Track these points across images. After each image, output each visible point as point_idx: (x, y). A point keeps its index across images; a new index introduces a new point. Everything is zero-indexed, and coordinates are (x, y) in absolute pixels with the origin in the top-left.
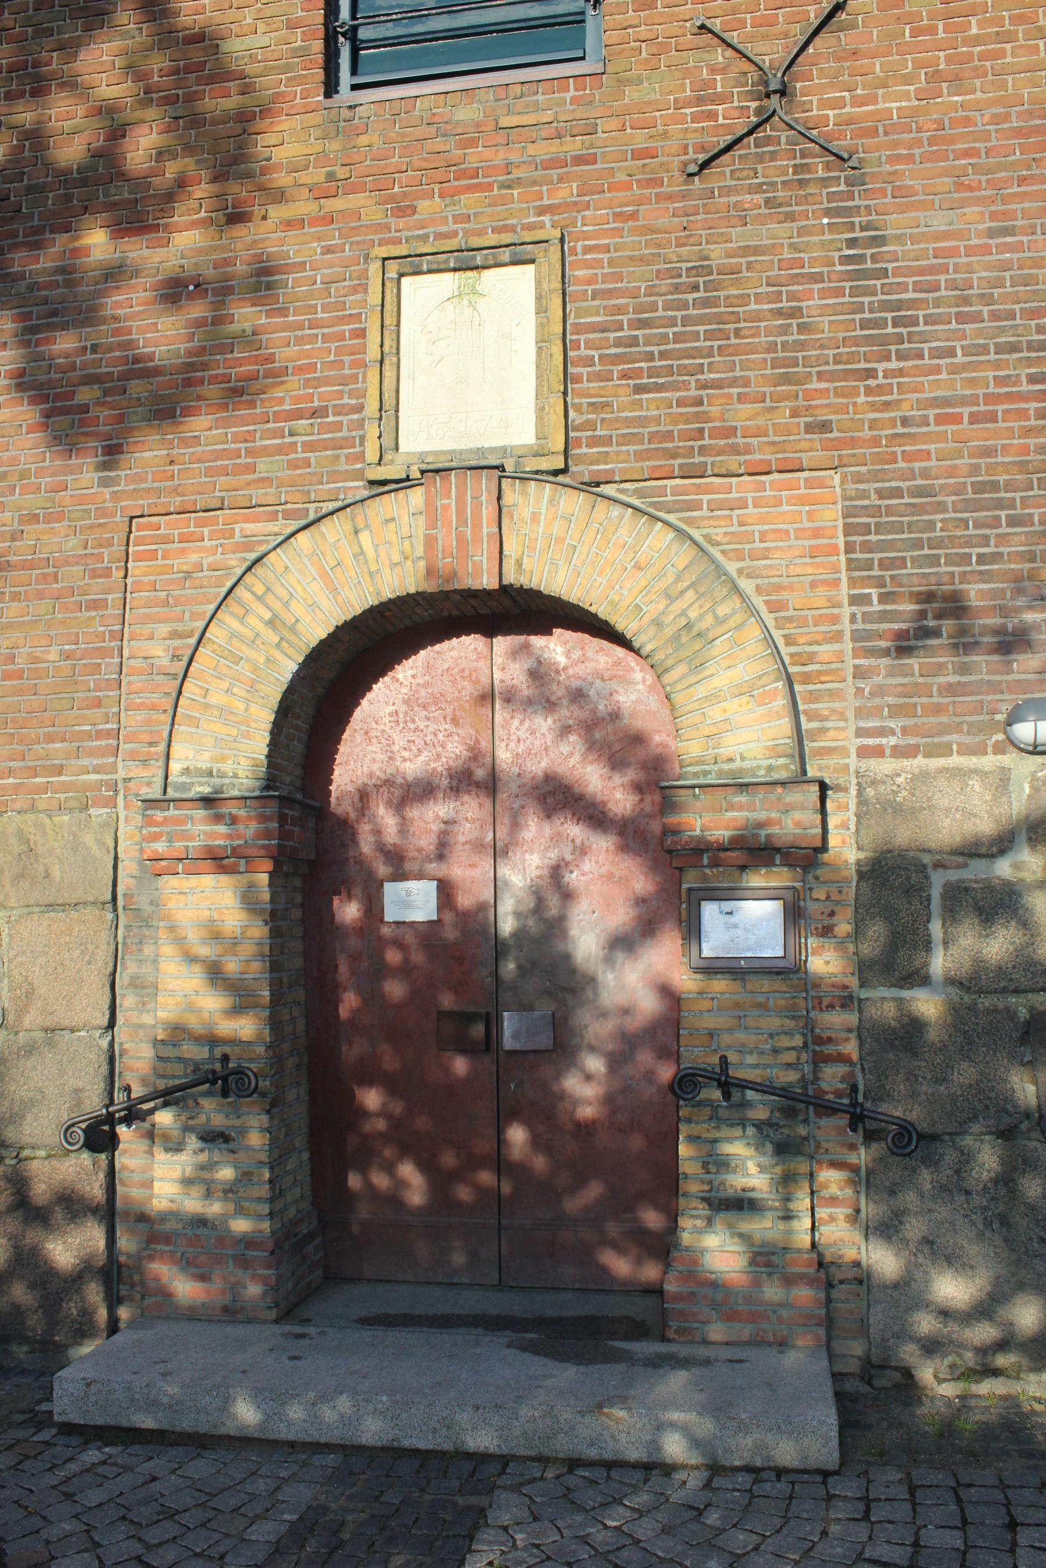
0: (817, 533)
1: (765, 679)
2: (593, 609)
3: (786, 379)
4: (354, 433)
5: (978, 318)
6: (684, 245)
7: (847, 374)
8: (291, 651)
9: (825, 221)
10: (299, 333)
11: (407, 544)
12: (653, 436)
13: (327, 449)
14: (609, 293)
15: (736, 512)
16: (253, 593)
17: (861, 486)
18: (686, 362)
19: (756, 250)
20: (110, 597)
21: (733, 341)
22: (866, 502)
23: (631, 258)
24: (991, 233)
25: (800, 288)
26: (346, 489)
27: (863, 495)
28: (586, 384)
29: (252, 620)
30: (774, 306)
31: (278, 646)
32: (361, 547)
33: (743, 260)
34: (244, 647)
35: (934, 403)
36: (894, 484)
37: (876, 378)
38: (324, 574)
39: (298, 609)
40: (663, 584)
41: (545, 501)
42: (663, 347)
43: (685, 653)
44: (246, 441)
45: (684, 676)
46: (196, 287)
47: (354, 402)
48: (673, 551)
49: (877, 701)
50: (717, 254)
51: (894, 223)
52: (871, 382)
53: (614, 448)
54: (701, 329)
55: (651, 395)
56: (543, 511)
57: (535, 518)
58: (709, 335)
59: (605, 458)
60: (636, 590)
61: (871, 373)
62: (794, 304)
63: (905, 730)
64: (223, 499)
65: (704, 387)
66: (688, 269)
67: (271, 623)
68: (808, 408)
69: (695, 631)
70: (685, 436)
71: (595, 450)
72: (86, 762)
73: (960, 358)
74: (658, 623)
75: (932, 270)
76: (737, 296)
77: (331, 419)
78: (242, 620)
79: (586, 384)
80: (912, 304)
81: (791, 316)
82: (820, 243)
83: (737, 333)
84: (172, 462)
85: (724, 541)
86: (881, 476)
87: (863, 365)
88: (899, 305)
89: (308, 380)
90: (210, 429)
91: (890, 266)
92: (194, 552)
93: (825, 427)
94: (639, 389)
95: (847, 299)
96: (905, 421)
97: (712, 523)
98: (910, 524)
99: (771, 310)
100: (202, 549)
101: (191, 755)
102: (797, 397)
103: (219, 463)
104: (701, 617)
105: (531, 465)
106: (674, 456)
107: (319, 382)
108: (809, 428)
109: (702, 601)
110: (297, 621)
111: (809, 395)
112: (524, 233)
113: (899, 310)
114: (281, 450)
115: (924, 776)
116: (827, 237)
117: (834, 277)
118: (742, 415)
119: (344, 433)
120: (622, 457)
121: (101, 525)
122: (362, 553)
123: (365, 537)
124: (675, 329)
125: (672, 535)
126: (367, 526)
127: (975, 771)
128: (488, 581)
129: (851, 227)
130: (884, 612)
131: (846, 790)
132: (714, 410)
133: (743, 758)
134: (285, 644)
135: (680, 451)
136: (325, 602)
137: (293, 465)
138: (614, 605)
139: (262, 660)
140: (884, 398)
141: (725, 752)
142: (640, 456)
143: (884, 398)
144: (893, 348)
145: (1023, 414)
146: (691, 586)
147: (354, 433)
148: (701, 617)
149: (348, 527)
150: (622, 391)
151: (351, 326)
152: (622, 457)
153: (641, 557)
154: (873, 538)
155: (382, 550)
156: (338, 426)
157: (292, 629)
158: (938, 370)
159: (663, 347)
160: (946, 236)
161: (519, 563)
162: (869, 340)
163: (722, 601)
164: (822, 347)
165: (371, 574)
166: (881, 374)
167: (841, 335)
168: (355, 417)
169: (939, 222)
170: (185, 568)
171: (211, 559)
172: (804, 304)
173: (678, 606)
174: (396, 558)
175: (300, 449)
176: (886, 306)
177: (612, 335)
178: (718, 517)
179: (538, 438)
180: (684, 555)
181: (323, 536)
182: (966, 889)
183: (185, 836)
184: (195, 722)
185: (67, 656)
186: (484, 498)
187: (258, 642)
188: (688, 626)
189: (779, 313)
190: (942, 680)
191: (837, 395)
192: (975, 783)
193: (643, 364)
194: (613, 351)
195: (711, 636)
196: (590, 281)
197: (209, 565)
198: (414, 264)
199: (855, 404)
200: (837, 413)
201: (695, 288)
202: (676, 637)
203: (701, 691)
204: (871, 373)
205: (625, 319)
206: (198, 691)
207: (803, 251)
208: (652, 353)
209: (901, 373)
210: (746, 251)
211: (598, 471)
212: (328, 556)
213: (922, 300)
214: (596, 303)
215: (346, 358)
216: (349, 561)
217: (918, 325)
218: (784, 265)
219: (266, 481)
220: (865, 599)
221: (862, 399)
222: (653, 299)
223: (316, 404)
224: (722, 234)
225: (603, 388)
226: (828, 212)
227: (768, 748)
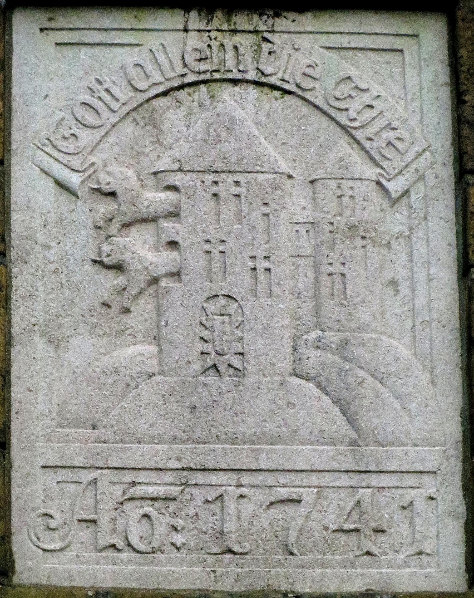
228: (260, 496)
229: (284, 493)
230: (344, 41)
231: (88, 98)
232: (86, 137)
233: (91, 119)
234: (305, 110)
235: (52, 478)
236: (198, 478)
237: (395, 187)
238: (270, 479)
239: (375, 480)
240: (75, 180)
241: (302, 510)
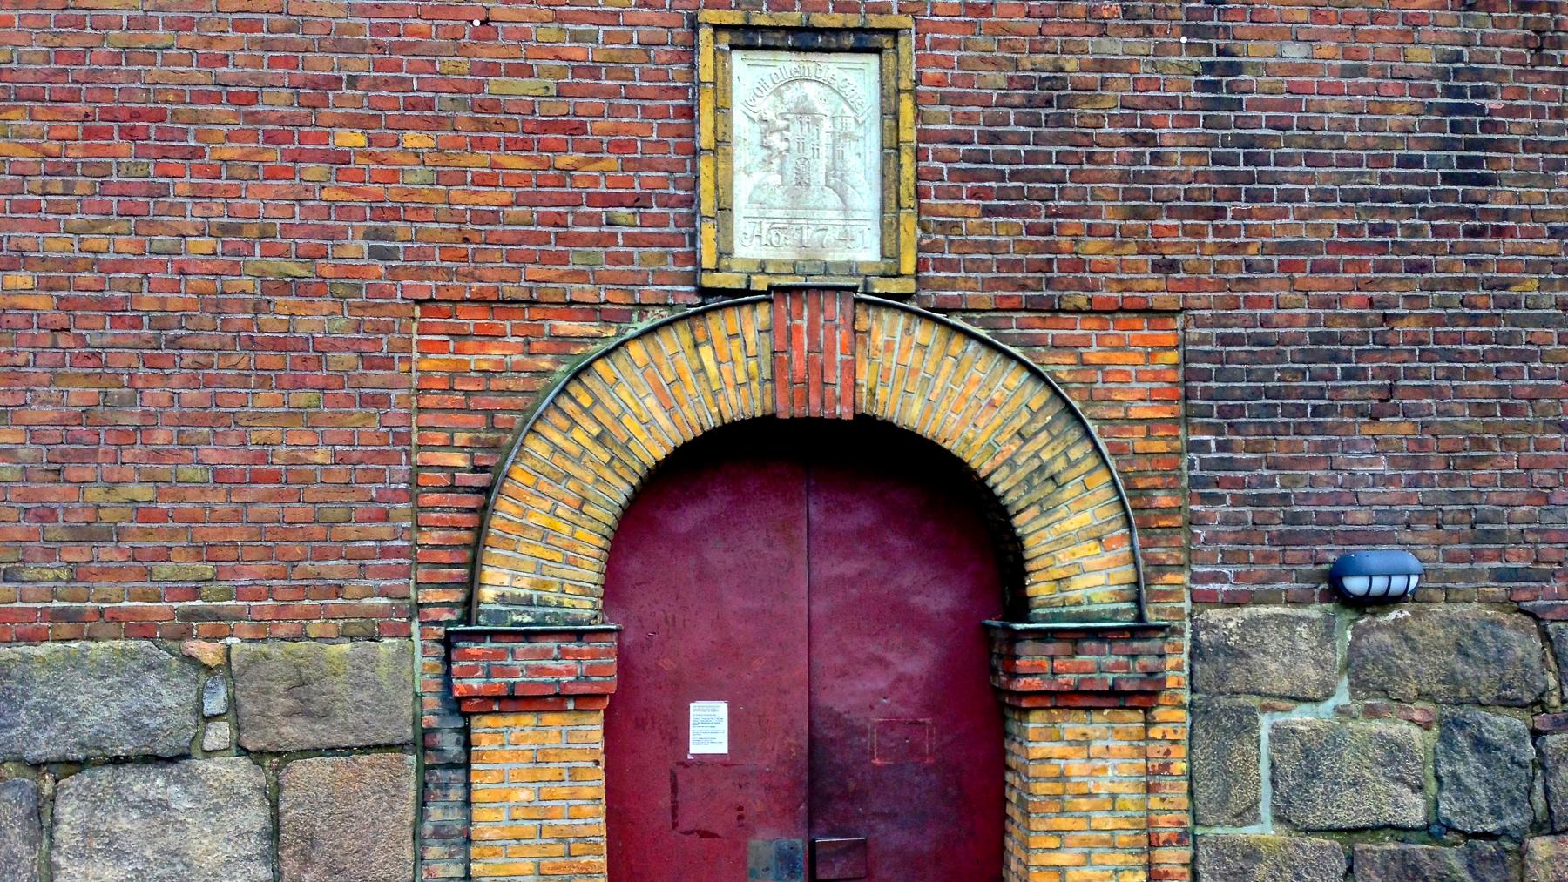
0: (1157, 376)
1: (1113, 525)
2: (946, 446)
3: (1137, 213)
4: (683, 230)
5: (1324, 161)
6: (1039, 52)
7: (1196, 213)
8: (624, 473)
9: (1184, 40)
10: (615, 102)
11: (752, 363)
12: (1001, 265)
13: (651, 245)
14: (960, 100)
17: (1204, 331)
18: (1038, 185)
19: (1113, 66)
20: (393, 393)
21: (1086, 167)
22: (1207, 348)
23: (983, 59)
24: (1345, 72)
25: (1155, 113)
26: (674, 293)
27: (1204, 340)
28: (934, 201)
29: (578, 434)
30: (1128, 131)
31: (608, 465)
32: (701, 362)
33: (1098, 76)
34: (568, 464)
35: (1281, 248)
36: (1236, 330)
37: (1225, 218)
38: (658, 391)
40: (1017, 424)
41: (900, 329)
42: (1015, 167)
43: (1036, 495)
44: (556, 225)
45: (1035, 518)
46: (482, 23)
47: (682, 193)
49: (1211, 548)
50: (1071, 64)
51: (1253, 51)
52: (1219, 222)
53: (963, 274)
54: (1053, 149)
55: (1001, 219)
56: (898, 339)
57: (889, 346)
59: (951, 284)
60: (990, 428)
62: (1149, 130)
63: (1237, 575)
64: (531, 291)
65: (1055, 215)
66: (1043, 80)
67: (598, 439)
68: (1157, 245)
69: (1047, 474)
70: (1034, 267)
71: (942, 274)
72: (371, 583)
73: (1307, 205)
74: (1011, 463)
75: (1283, 106)
76: (1090, 116)
77: (655, 210)
78: (564, 432)
79: (934, 201)
80: (1264, 141)
81: (1144, 144)
82: (1179, 67)
83: (1090, 157)
84: (466, 240)
86: (1223, 321)
87: (1211, 204)
88: (1251, 142)
89: (628, 160)
90: (512, 205)
91: (1245, 97)
93: (1172, 266)
94: (988, 211)
95: (1200, 130)
96: (1249, 267)
98: (1249, 372)
99: (1125, 135)
100: (506, 346)
101: (507, 581)
102: (1146, 234)
103: (524, 247)
104: (1054, 459)
105: (881, 286)
106: (1024, 287)
107: (640, 165)
108: (1156, 267)
111: (1157, 231)
112: (871, 16)
113: (1252, 146)
114: (598, 240)
115: (1253, 623)
116: (1184, 58)
117: (1189, 104)
118: (1092, 247)
119: (672, 229)
120: (971, 284)
121: (376, 305)
122: (703, 369)
123: (706, 352)
124: (1027, 148)
125: (1026, 374)
126: (709, 340)
127: (1303, 619)
128: (844, 412)
129: (1208, 50)
130: (1222, 459)
131: (1181, 633)
132: (1064, 241)
133: (1090, 602)
134: (616, 463)
135: (1029, 282)
136: (662, 419)
137: (615, 259)
138: (968, 442)
139: (590, 479)
141: (1074, 595)
142: (988, 285)
144: (1243, 187)
145: (1360, 267)
146: (1046, 427)
147: (683, 230)
149: (686, 338)
150: (971, 212)
151: (676, 102)
152: (971, 284)
153: (996, 396)
154: (1213, 384)
155: (726, 367)
156: (662, 221)
157: (626, 448)
158: (1284, 214)
159: (1015, 167)
160: (1299, 70)
161: (872, 393)
162: (1223, 177)
163: (1074, 444)
164: (1174, 181)
165: (714, 394)
166: (1230, 214)
167: (1193, 169)
168: (684, 210)
169: (1295, 52)
170: (485, 366)
172: (1157, 131)
173: (1031, 447)
175: (621, 242)
176: (1240, 141)
177: (962, 148)
179: (883, 256)
180: (1038, 396)
181: (658, 346)
182: (1293, 731)
183: (506, 672)
184: (504, 541)
185: (340, 460)
187: (585, 459)
188: (1041, 469)
189: (1133, 139)
190: (1273, 528)
191: (1185, 234)
192: (1302, 629)
193: (993, 184)
194: (963, 165)
196: (939, 83)
198: (747, 38)
199: (1202, 244)
200: (1185, 252)
201: (1049, 103)
202: (1028, 480)
203: (1050, 534)
204: (1220, 213)
205: (975, 129)
206: (514, 510)
207: (1160, 72)
208: (1003, 172)
209: (1249, 214)
210: (1103, 65)
211: (946, 297)
212: (665, 372)
213: (1276, 138)
214: (946, 108)
215: (671, 140)
216: (689, 377)
217: (1268, 164)
218: (1140, 86)
219: (580, 276)
220: (1202, 446)
221: (1210, 239)
222: (1005, 110)
223: (638, 190)
224: (1078, 43)
225: (953, 206)
226: (1186, 31)
227: (1114, 592)
240: (755, 117)
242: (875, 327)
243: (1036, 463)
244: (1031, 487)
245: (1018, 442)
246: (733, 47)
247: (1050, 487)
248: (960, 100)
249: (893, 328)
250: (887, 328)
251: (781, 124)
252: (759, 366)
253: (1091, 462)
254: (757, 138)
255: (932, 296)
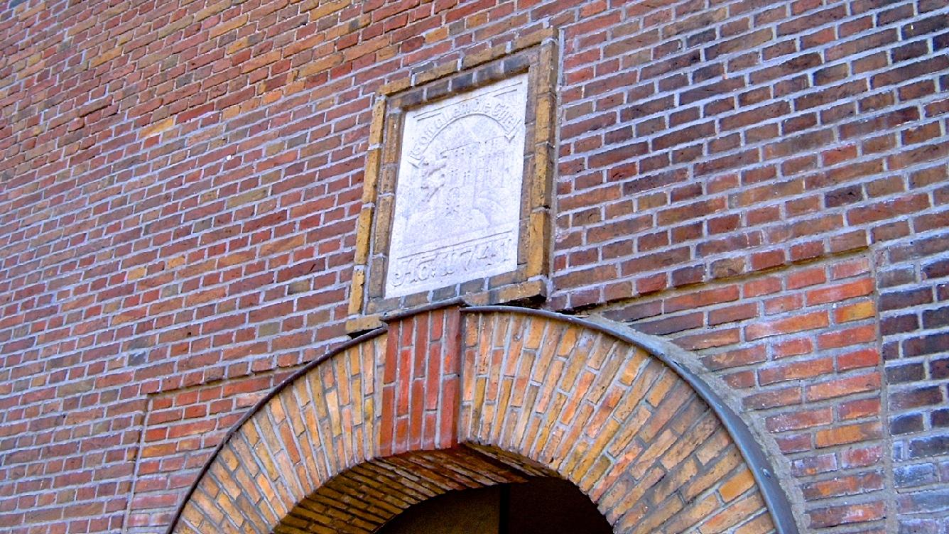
14: (605, 85)
15: (743, 324)
16: (226, 468)
25: (814, 31)
29: (222, 501)
32: (327, 410)
39: (264, 484)
40: (635, 425)
48: (648, 382)
52: (910, 126)
56: (506, 348)
58: (709, 110)
60: (603, 438)
61: (909, 114)
67: (237, 504)
69: (672, 486)
85: (727, 363)
92: (196, 428)
95: (875, 30)
97: (714, 341)
104: (680, 466)
109: (680, 445)
110: (261, 499)
125: (646, 361)
126: (335, 384)
135: (674, 255)
138: (577, 458)
140: (928, 142)
143: (928, 142)
148: (680, 466)
165: (334, 441)
171: (208, 435)
173: (651, 454)
174: (358, 420)
177: (602, 132)
178: (721, 332)
186: (443, 340)
195: (691, 493)
197: (207, 441)
202: (648, 497)
228: (459, 253)
229: (465, 250)
230: (500, 92)
231: (423, 136)
232: (423, 148)
233: (424, 141)
234: (487, 119)
235: (400, 262)
236: (442, 251)
237: (509, 137)
238: (462, 246)
239: (493, 238)
240: (417, 162)
241: (471, 254)
242: (483, 338)
243: (658, 473)
244: (651, 510)
245: (637, 451)
246: (406, 109)
247: (676, 506)
248: (605, 85)
249: (500, 338)
250: (497, 341)
251: (442, 161)
252: (374, 404)
253: (726, 464)
254: (418, 183)
255: (568, 296)
